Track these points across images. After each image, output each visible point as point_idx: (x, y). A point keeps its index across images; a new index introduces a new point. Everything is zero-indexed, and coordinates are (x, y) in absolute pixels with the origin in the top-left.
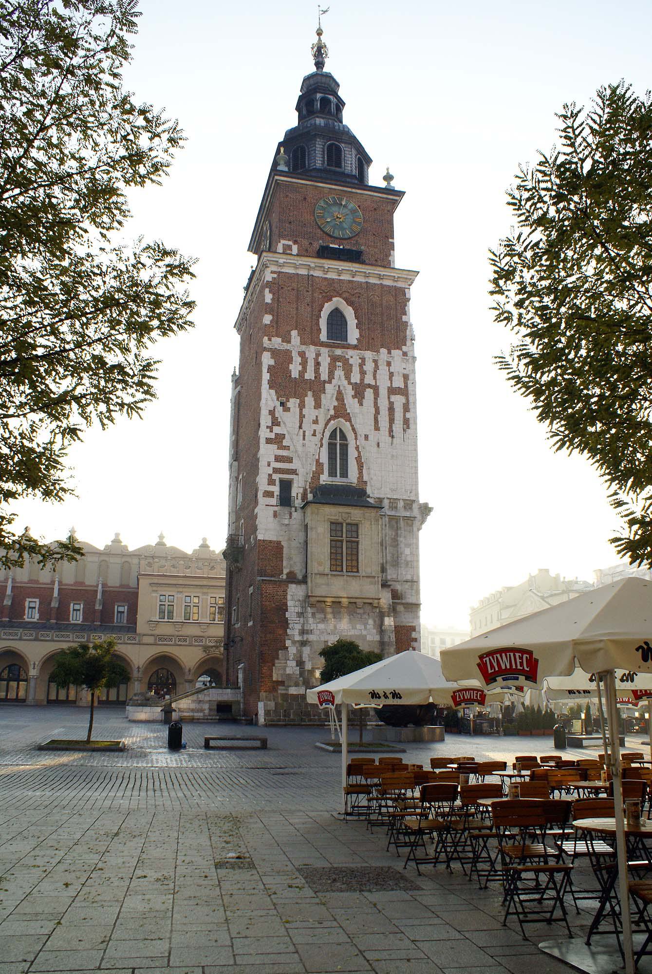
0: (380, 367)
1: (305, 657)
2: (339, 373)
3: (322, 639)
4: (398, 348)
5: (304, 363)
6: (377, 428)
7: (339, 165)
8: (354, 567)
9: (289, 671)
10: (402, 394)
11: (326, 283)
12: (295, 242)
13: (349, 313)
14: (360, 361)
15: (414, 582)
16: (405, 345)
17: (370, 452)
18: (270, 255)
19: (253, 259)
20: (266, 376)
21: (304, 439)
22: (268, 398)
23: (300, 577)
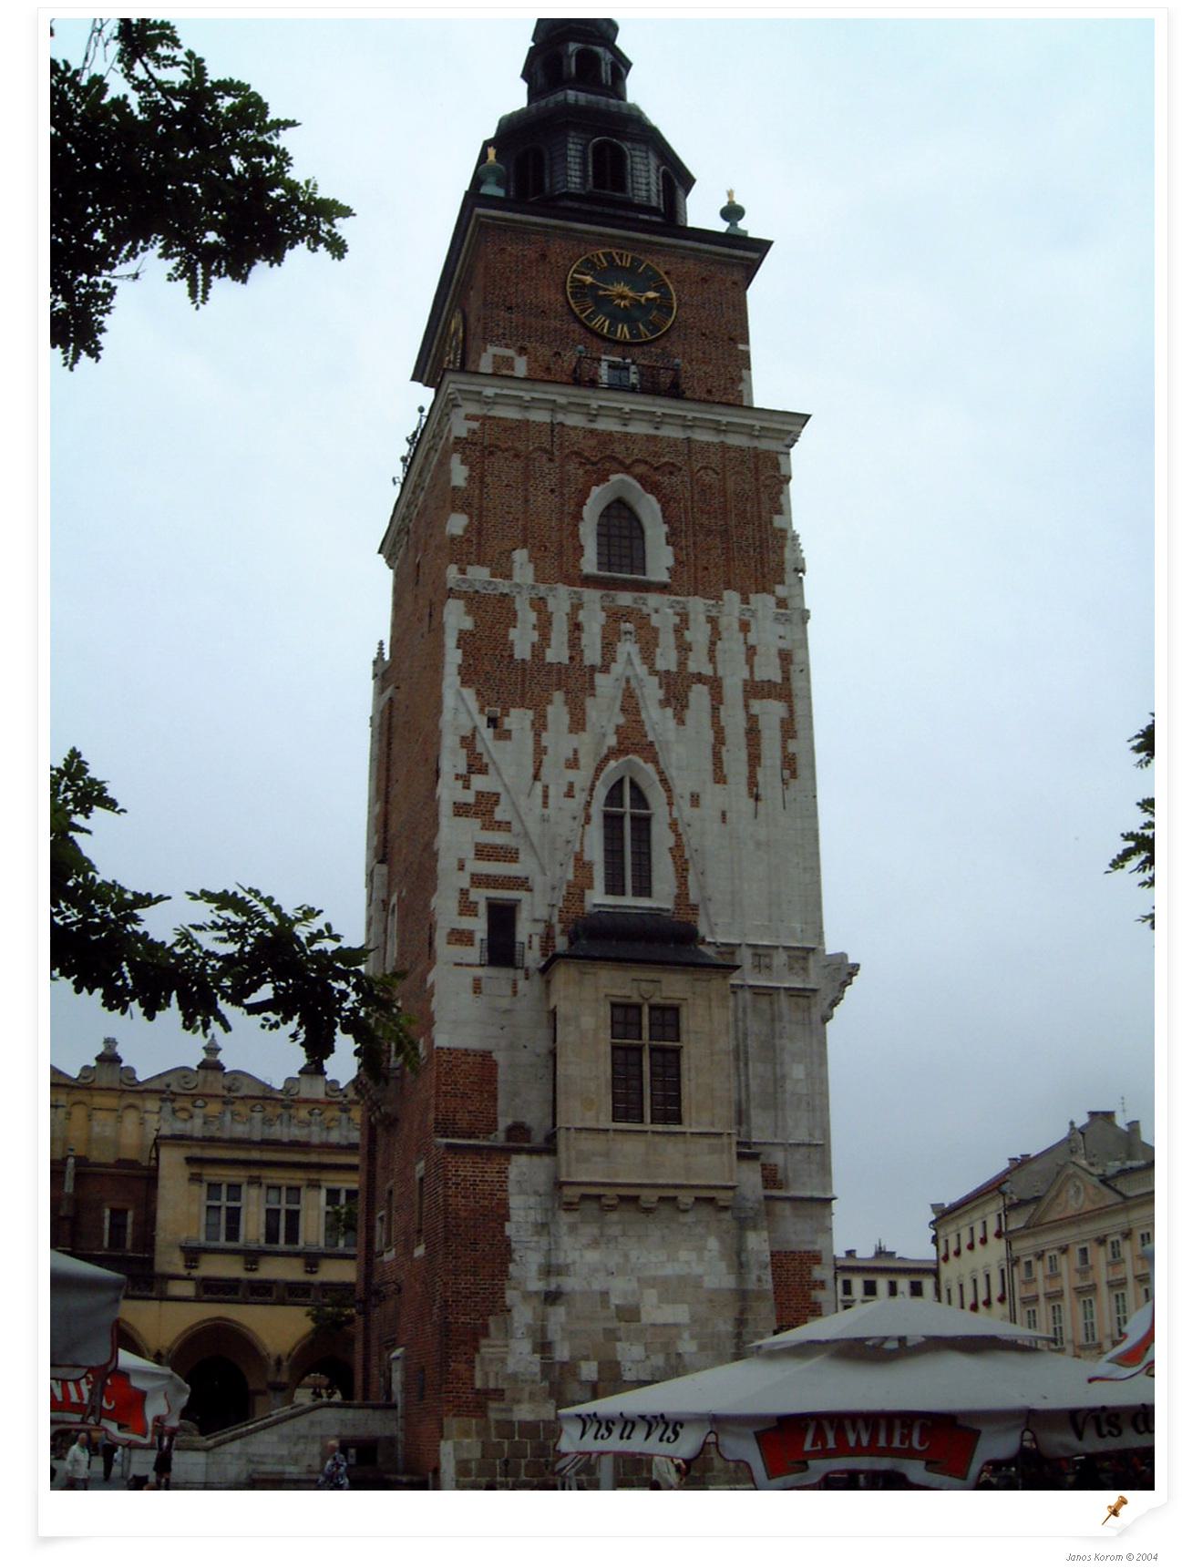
0: (724, 635)
1: (554, 1334)
2: (627, 648)
3: (596, 1286)
4: (764, 590)
5: (544, 625)
6: (720, 778)
7: (621, 187)
8: (669, 1110)
9: (512, 1365)
10: (779, 697)
11: (593, 442)
12: (522, 351)
13: (649, 509)
14: (677, 620)
15: (819, 1150)
16: (782, 582)
17: (704, 833)
18: (462, 378)
19: (426, 395)
20: (453, 657)
21: (545, 804)
22: (459, 707)
23: (538, 1139)
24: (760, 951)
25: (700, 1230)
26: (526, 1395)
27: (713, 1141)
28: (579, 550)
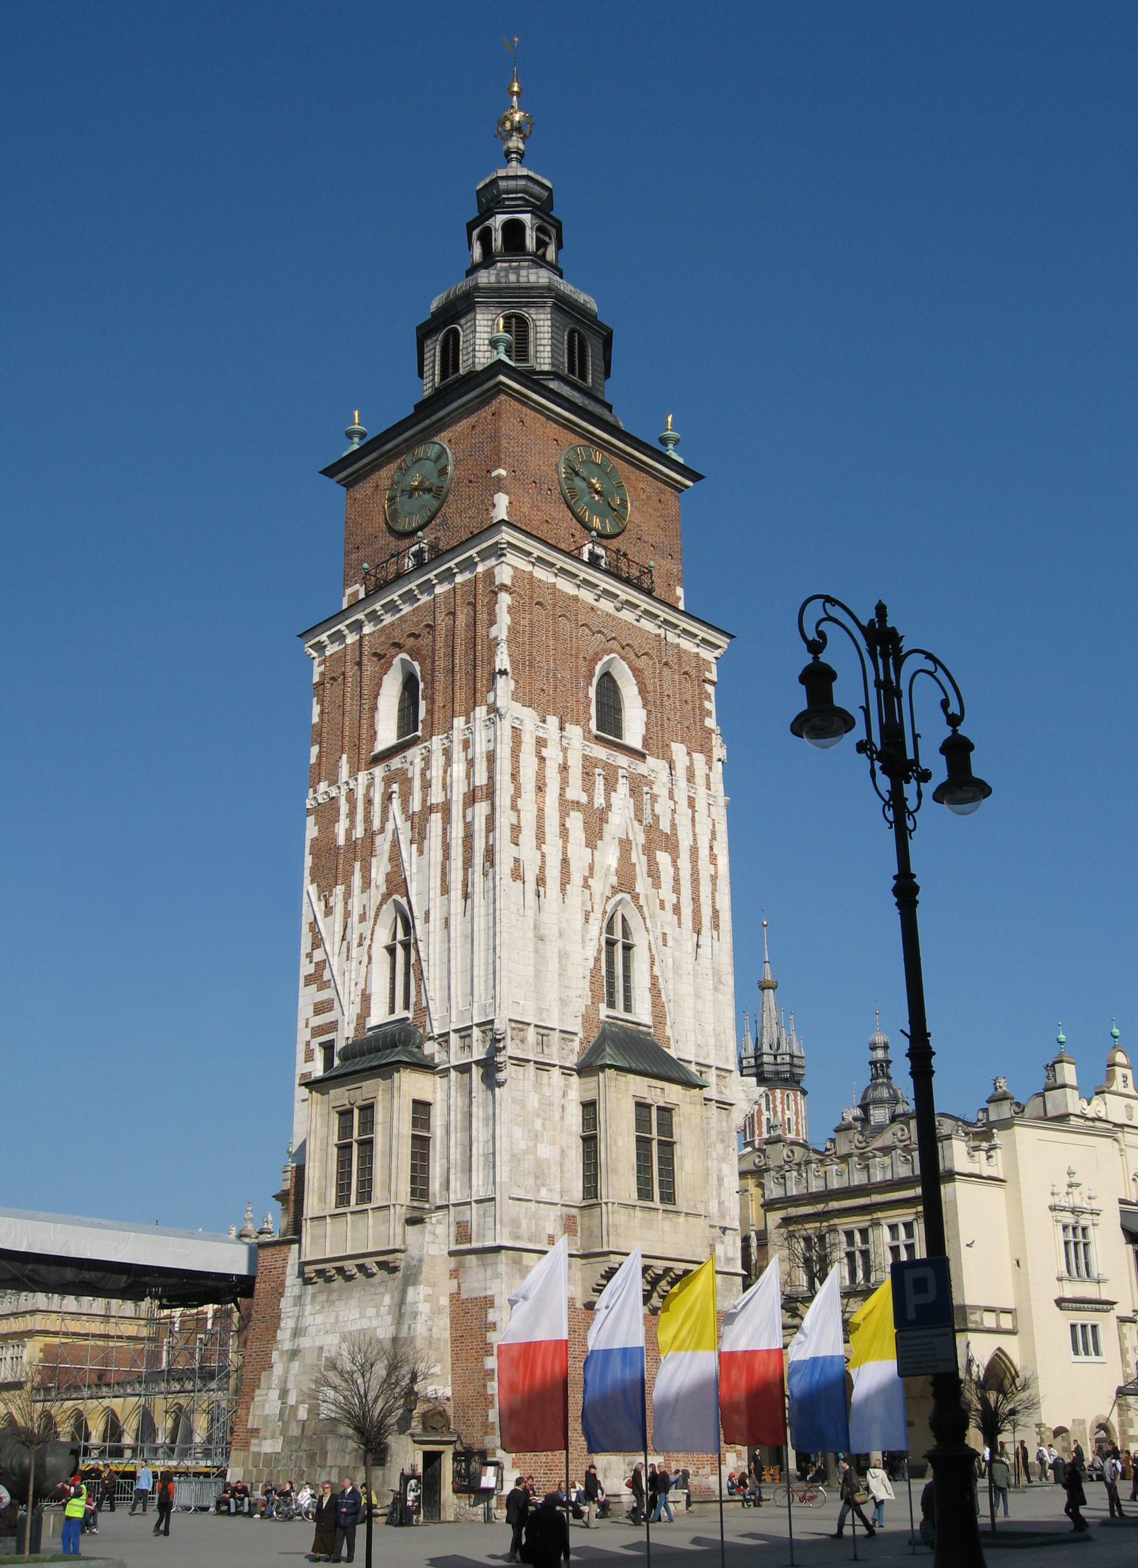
1: (290, 1385)
2: (396, 804)
3: (317, 1344)
6: (445, 890)
8: (365, 1195)
9: (267, 1411)
11: (383, 639)
24: (463, 1034)
25: (382, 1289)
26: (268, 1434)
27: (386, 1212)
28: (373, 736)
